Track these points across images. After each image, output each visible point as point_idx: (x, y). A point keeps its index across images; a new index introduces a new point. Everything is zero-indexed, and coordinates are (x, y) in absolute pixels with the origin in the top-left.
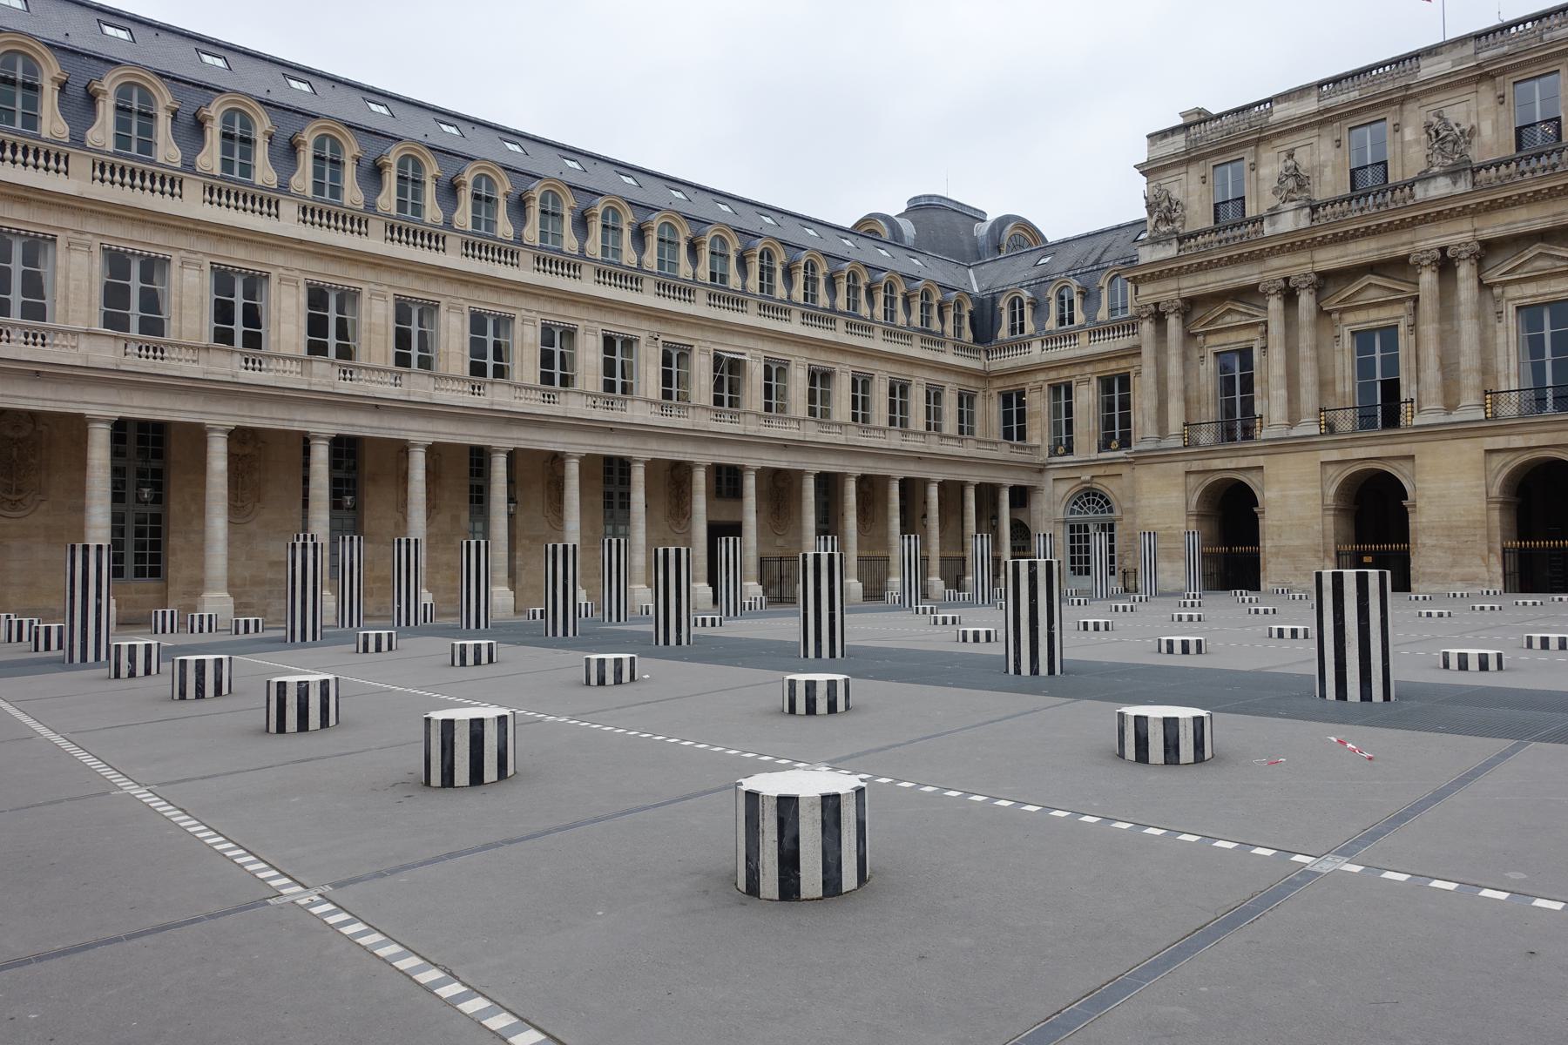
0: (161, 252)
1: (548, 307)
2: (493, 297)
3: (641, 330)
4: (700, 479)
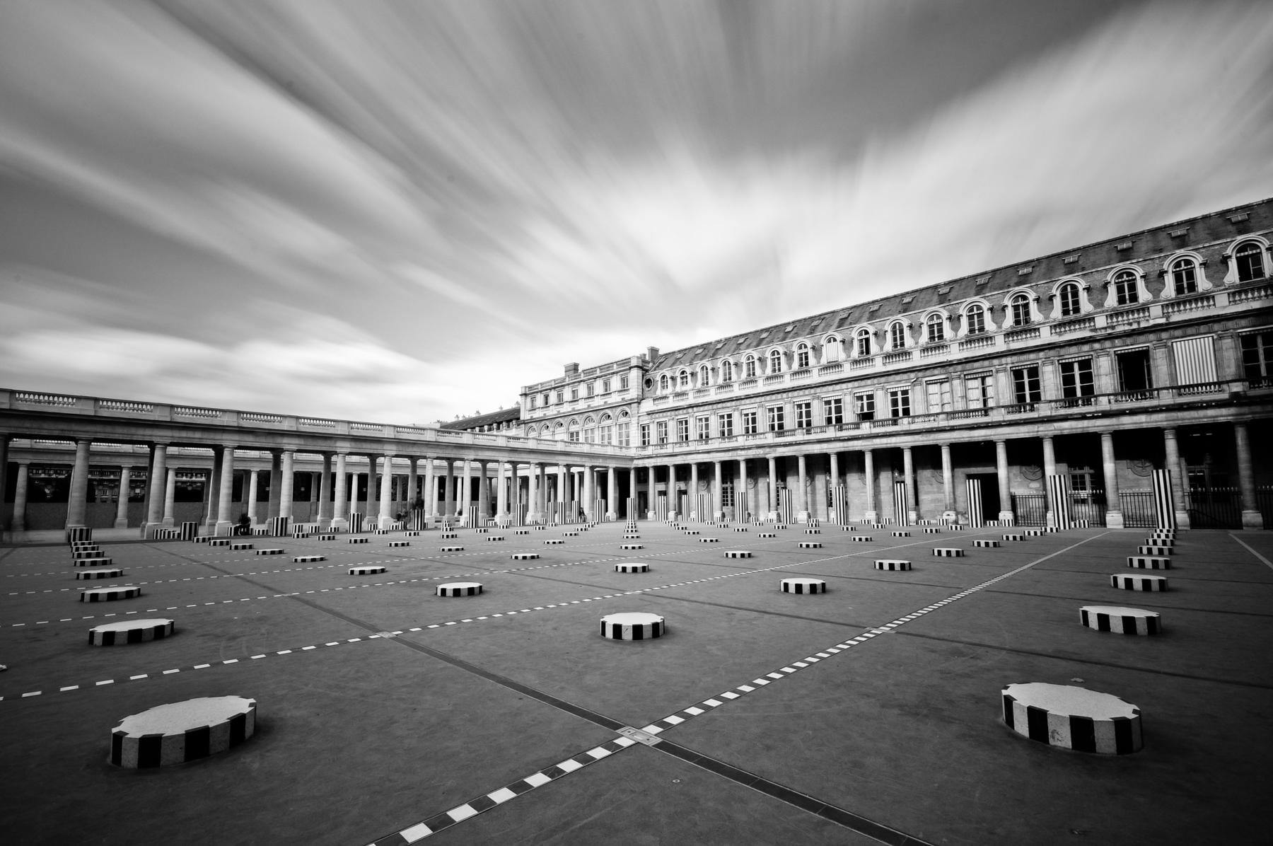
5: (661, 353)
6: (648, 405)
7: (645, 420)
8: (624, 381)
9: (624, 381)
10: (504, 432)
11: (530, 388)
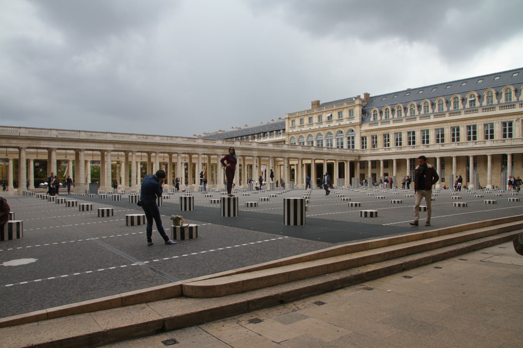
0: (413, 130)
1: (485, 120)
2: (471, 121)
3: (513, 119)
4: (489, 159)
5: (370, 96)
6: (366, 127)
7: (363, 134)
8: (351, 112)
9: (351, 112)
10: (268, 139)
11: (291, 114)
